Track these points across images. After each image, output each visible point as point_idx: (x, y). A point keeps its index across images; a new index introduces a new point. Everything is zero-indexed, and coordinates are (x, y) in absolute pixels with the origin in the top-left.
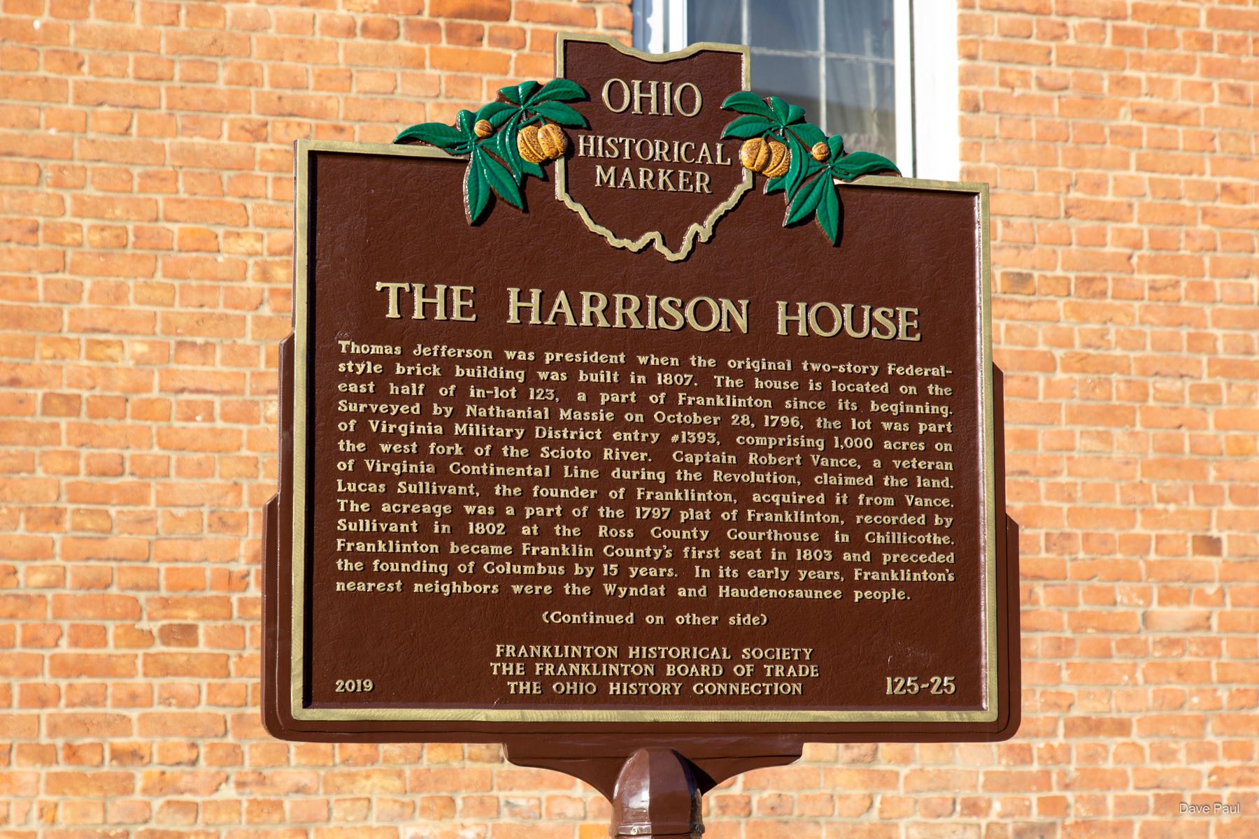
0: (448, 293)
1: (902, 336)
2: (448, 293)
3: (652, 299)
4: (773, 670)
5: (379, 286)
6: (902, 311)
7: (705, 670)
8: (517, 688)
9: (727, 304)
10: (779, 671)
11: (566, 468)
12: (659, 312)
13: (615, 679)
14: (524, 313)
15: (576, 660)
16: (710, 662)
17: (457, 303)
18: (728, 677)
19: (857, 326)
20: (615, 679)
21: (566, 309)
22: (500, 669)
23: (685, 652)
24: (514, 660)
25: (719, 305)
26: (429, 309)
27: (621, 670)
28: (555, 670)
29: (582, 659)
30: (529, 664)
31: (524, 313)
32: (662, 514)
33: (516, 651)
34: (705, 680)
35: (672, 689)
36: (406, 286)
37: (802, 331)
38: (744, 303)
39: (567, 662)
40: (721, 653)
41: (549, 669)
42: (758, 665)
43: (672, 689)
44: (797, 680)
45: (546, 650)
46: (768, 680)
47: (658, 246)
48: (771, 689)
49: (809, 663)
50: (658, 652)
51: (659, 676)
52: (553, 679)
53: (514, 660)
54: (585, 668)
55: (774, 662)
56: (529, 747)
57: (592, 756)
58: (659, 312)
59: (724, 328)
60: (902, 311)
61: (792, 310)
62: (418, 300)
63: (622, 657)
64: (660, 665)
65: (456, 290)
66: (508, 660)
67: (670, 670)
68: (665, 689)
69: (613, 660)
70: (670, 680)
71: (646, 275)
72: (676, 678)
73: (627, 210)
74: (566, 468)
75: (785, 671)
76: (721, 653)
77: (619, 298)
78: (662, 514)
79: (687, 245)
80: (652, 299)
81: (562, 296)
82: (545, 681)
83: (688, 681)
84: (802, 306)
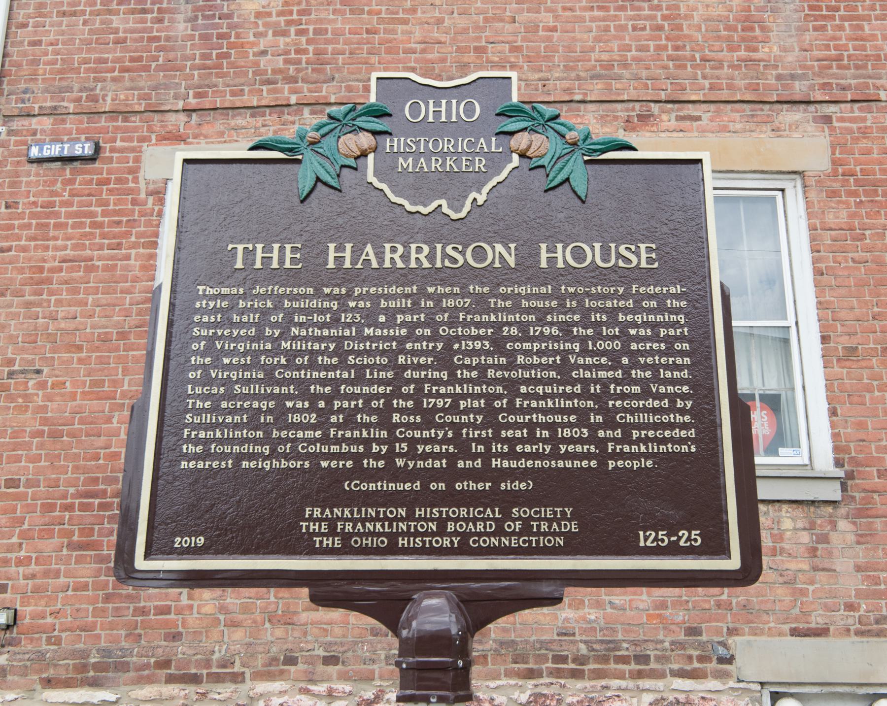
0: (282, 249)
1: (644, 264)
2: (282, 249)
3: (439, 247)
4: (539, 527)
5: (230, 247)
6: (643, 247)
7: (480, 527)
8: (321, 542)
9: (499, 248)
10: (544, 527)
11: (368, 371)
12: (445, 255)
13: (403, 534)
14: (339, 260)
15: (371, 520)
16: (484, 520)
17: (288, 255)
18: (500, 532)
19: (606, 258)
20: (403, 534)
21: (372, 257)
22: (308, 527)
23: (463, 512)
24: (320, 520)
25: (493, 248)
26: (267, 260)
27: (409, 527)
28: (354, 528)
29: (377, 519)
30: (332, 523)
31: (339, 260)
32: (445, 403)
33: (322, 513)
34: (480, 535)
35: (452, 542)
36: (250, 247)
37: (560, 264)
38: (513, 246)
39: (363, 521)
40: (493, 512)
41: (349, 527)
42: (526, 522)
43: (452, 542)
44: (560, 534)
45: (347, 512)
46: (535, 534)
47: (445, 209)
48: (538, 542)
49: (570, 520)
50: (441, 512)
51: (442, 532)
52: (351, 535)
53: (320, 520)
54: (378, 526)
55: (540, 519)
56: (329, 591)
57: (385, 600)
58: (445, 255)
59: (497, 265)
60: (643, 247)
61: (551, 250)
62: (259, 254)
63: (410, 517)
64: (442, 523)
65: (288, 247)
66: (315, 520)
67: (450, 527)
68: (446, 542)
69: (402, 519)
70: (450, 535)
71: (438, 230)
72: (456, 533)
73: (421, 185)
74: (368, 371)
75: (550, 527)
76: (493, 512)
77: (413, 247)
78: (445, 403)
79: (467, 207)
80: (439, 247)
81: (369, 248)
82: (346, 537)
83: (465, 536)
84: (560, 246)
